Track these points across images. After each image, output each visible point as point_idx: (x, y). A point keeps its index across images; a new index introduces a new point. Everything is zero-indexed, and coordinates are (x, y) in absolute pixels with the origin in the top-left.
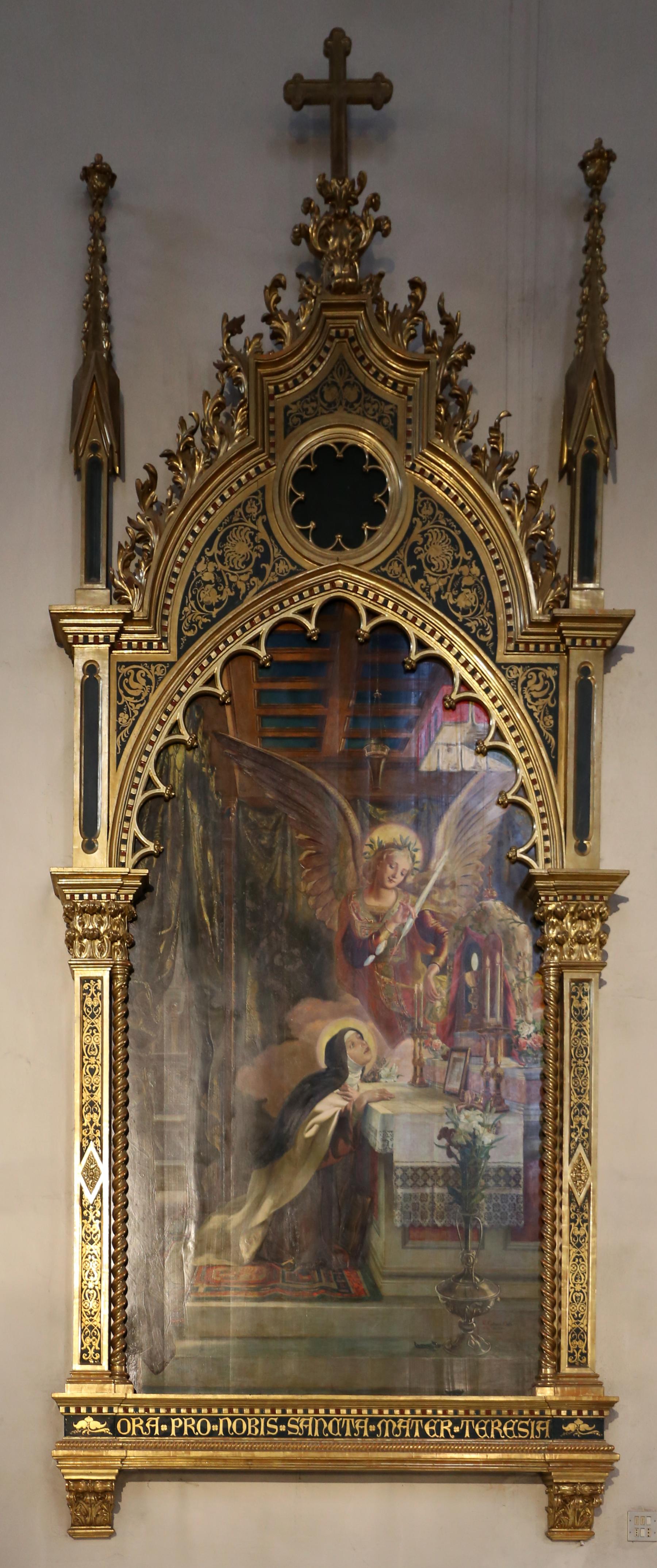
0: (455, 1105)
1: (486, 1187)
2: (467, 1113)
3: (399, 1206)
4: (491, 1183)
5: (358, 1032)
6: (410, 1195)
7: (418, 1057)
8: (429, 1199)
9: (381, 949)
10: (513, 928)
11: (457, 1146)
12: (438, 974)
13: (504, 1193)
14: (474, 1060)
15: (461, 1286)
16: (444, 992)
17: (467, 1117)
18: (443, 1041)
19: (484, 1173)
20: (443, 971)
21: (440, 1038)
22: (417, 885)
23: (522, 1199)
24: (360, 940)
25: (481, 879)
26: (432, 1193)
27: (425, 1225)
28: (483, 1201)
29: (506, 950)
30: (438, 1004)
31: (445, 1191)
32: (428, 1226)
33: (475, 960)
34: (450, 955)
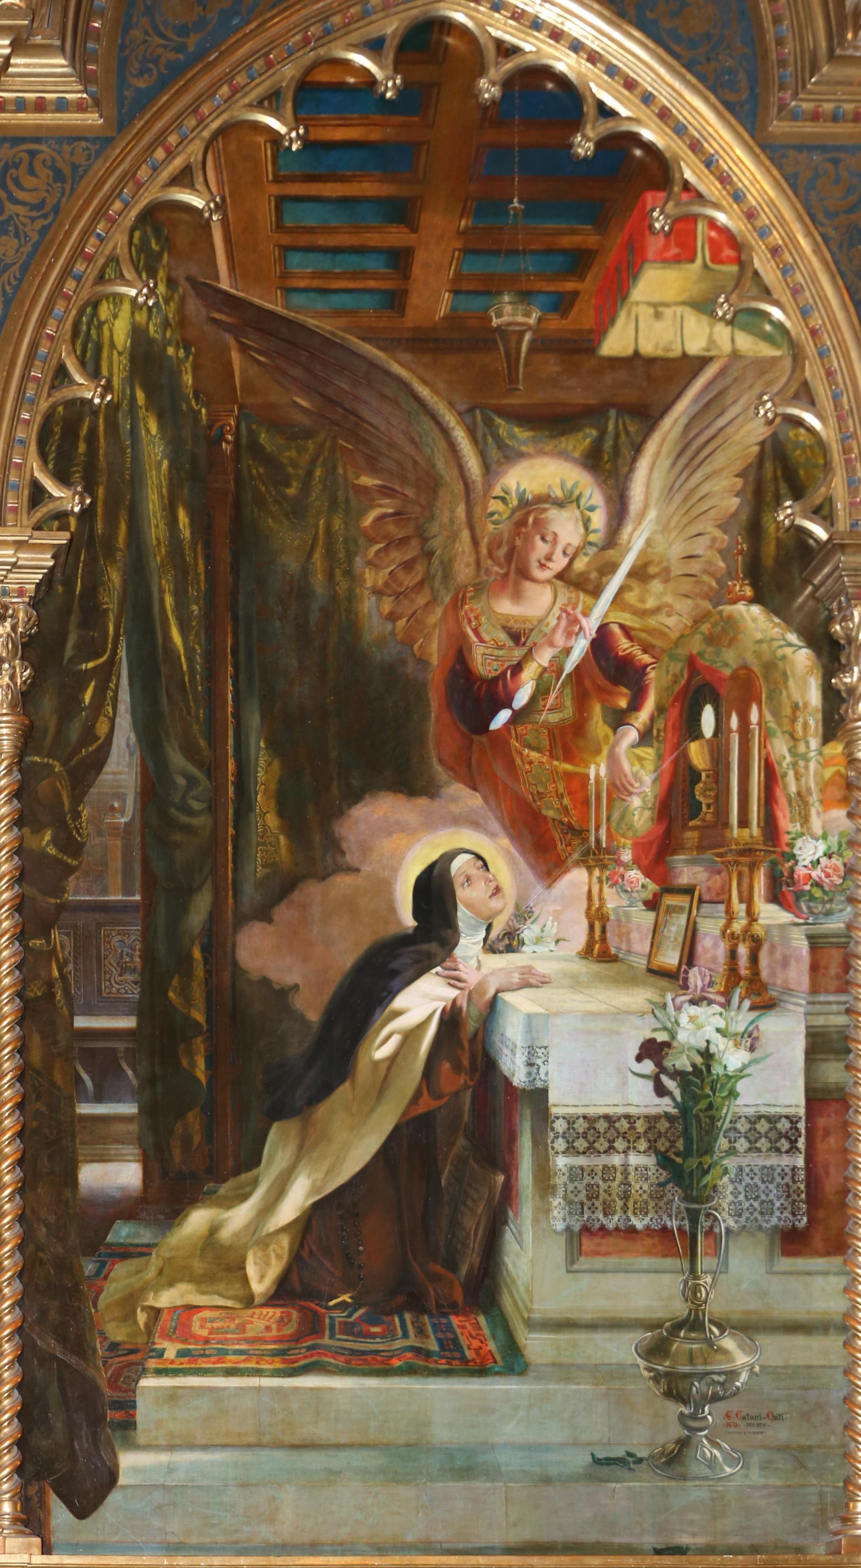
0: (669, 997)
1: (732, 1151)
2: (693, 1010)
3: (561, 1192)
4: (742, 1144)
5: (479, 857)
6: (582, 1169)
7: (596, 904)
8: (619, 1177)
9: (522, 698)
10: (784, 657)
11: (677, 1074)
12: (634, 746)
13: (768, 1163)
14: (706, 908)
16: (648, 779)
17: (692, 1019)
18: (647, 874)
19: (727, 1125)
20: (645, 737)
21: (640, 867)
22: (594, 575)
23: (802, 1175)
24: (484, 681)
25: (722, 564)
26: (625, 1166)
27: (611, 1226)
28: (725, 1179)
29: (770, 698)
31: (649, 1161)
32: (617, 1229)
33: (708, 718)
34: (660, 709)
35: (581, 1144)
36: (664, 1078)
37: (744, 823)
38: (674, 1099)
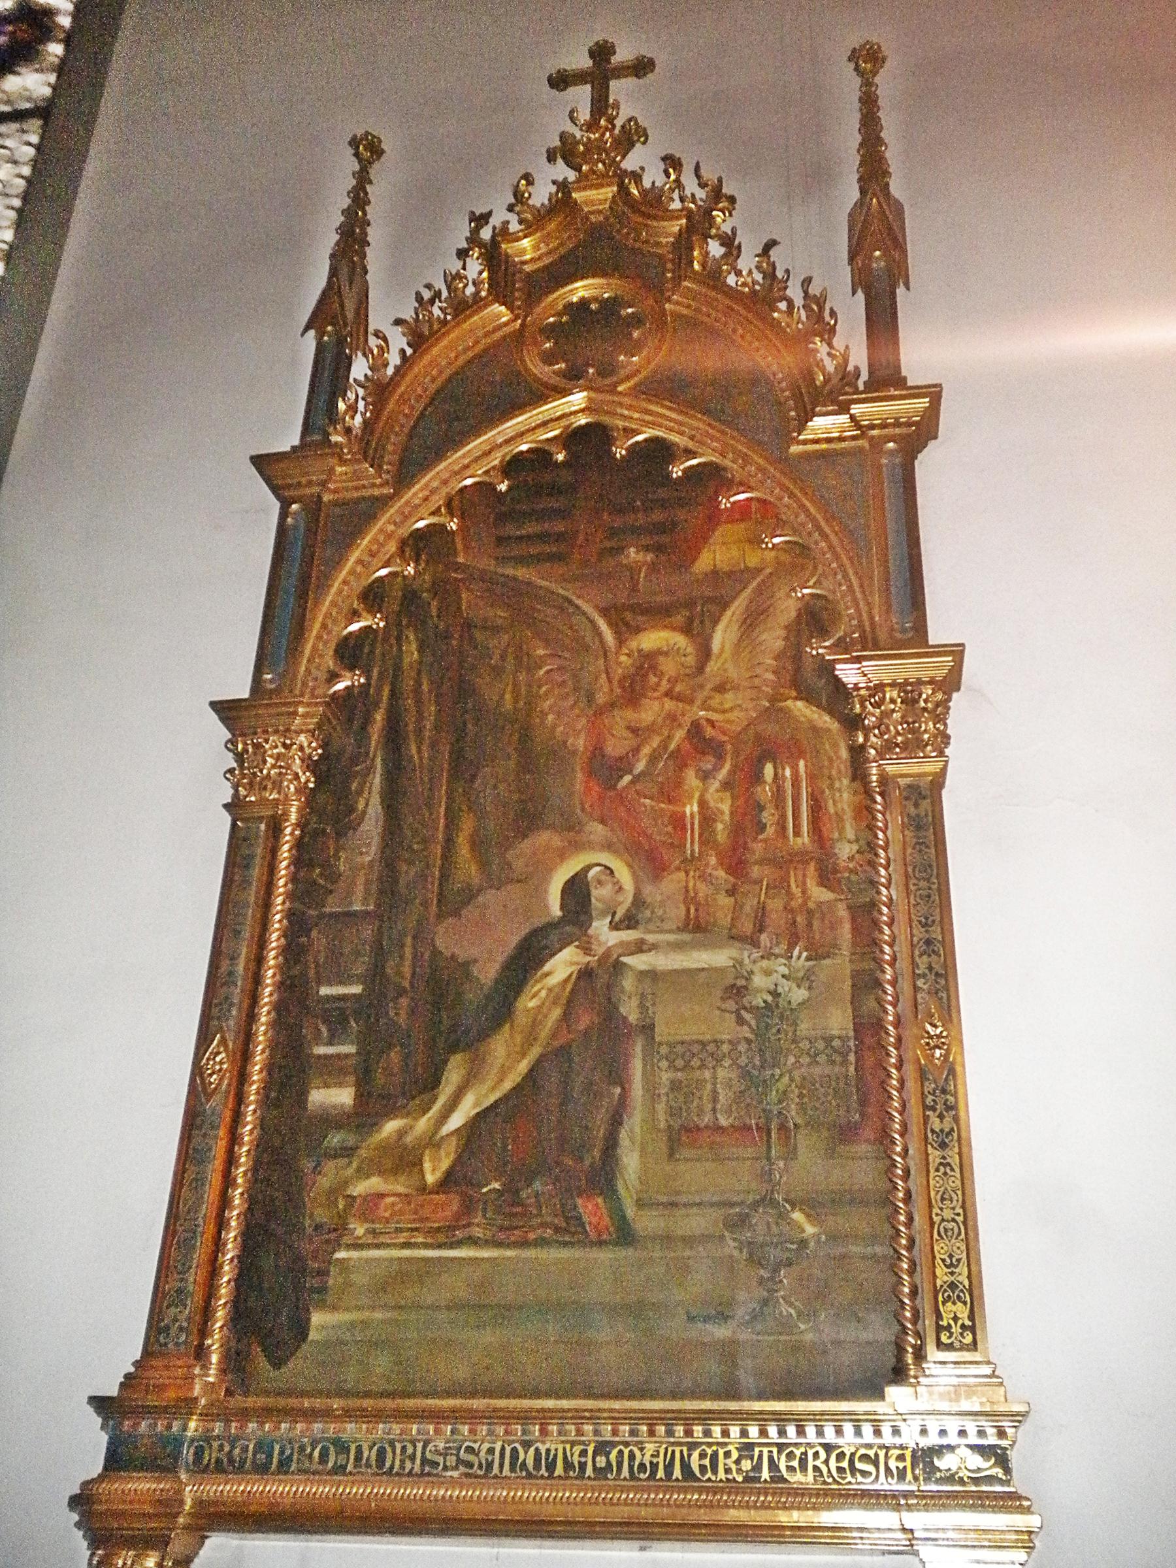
5: (609, 868)
11: (751, 1009)
15: (761, 1219)
20: (726, 785)
30: (720, 826)
32: (707, 1127)
33: (769, 770)
35: (680, 1063)
36: (743, 1012)
37: (797, 833)
38: (750, 1026)
